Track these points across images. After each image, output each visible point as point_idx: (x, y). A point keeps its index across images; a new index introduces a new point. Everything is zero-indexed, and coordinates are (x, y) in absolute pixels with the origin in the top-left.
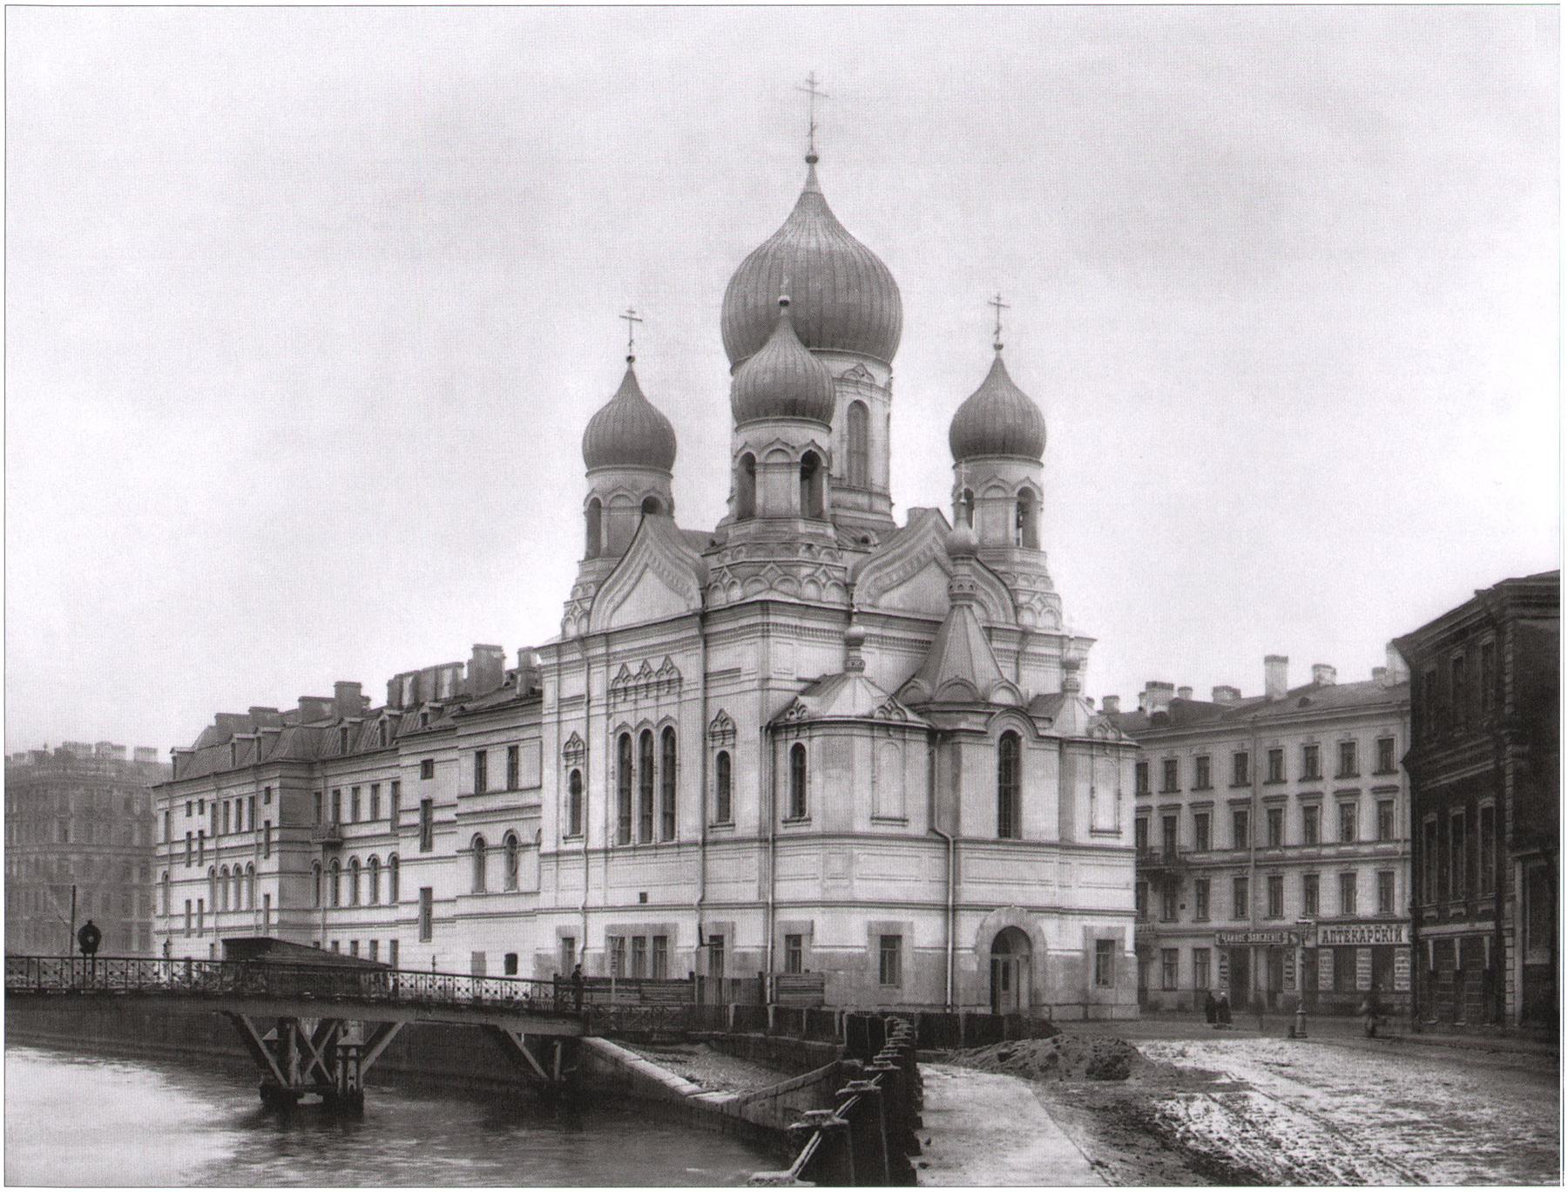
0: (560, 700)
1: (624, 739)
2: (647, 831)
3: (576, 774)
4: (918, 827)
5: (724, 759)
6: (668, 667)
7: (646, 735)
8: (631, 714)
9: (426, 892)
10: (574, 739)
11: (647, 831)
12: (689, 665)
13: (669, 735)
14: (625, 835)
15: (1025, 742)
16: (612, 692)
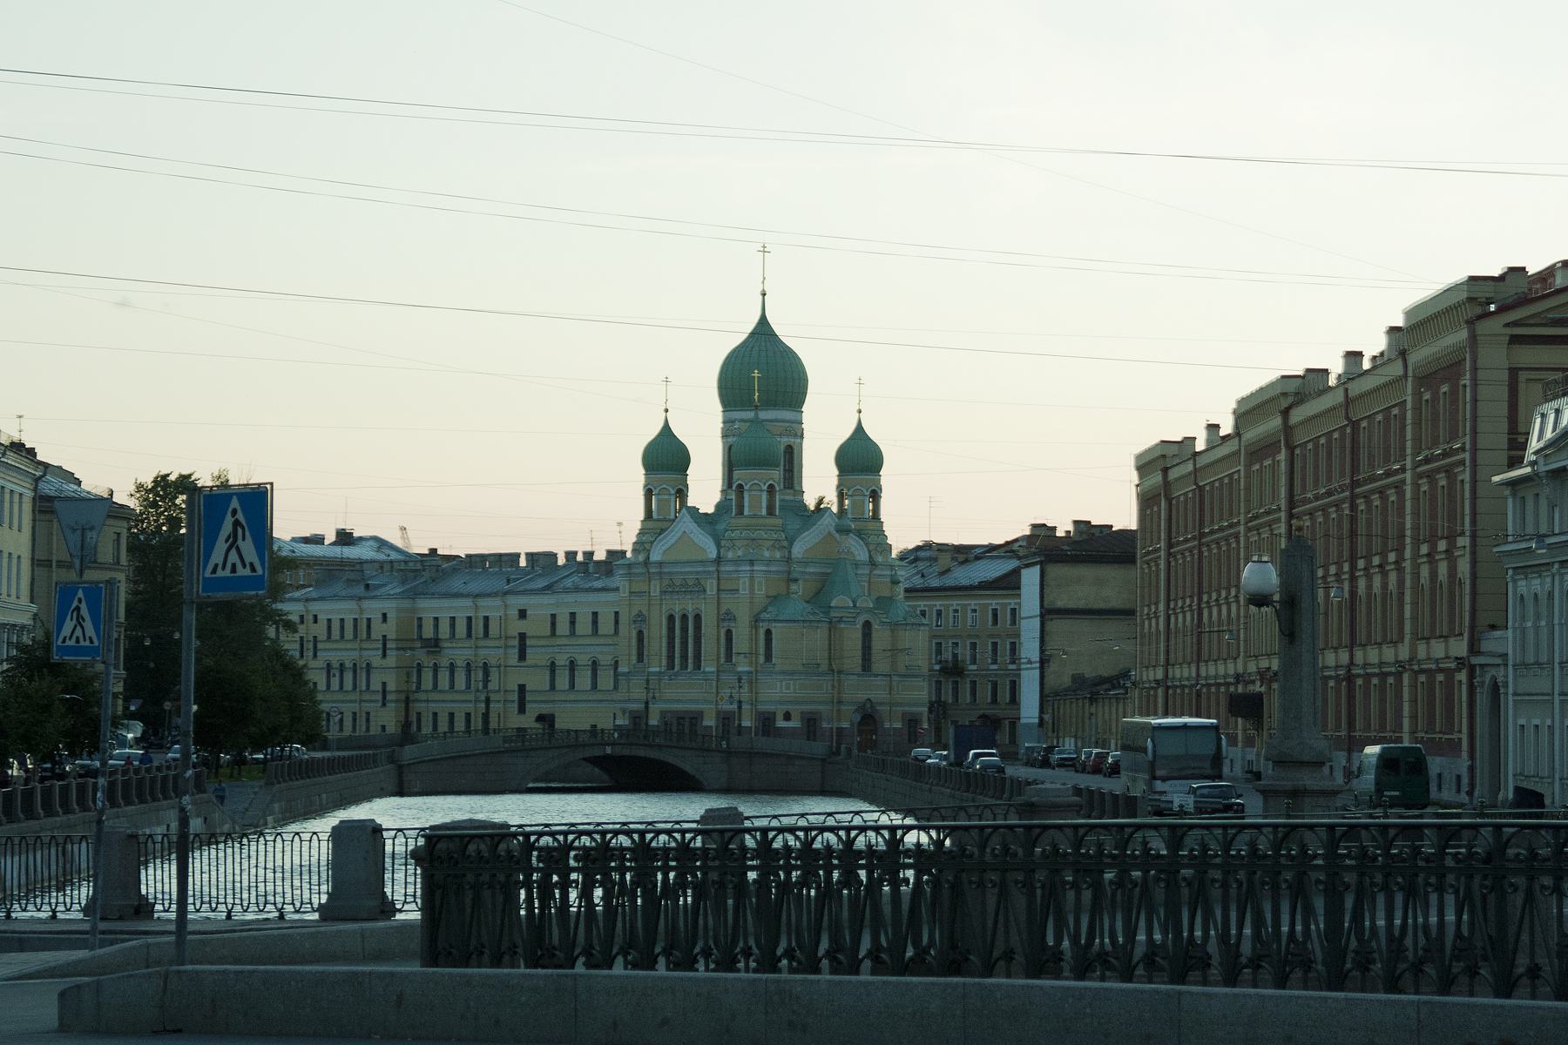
0: (630, 592)
1: (671, 618)
2: (684, 665)
3: (640, 633)
4: (824, 667)
5: (729, 632)
6: (698, 582)
7: (684, 617)
8: (678, 606)
9: (522, 688)
10: (640, 614)
11: (684, 665)
12: (711, 586)
13: (698, 618)
14: (671, 665)
15: (875, 626)
16: (663, 592)
